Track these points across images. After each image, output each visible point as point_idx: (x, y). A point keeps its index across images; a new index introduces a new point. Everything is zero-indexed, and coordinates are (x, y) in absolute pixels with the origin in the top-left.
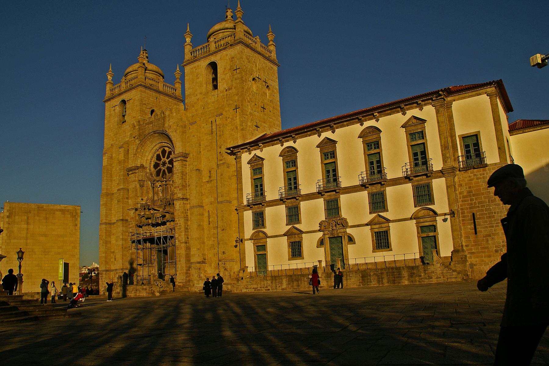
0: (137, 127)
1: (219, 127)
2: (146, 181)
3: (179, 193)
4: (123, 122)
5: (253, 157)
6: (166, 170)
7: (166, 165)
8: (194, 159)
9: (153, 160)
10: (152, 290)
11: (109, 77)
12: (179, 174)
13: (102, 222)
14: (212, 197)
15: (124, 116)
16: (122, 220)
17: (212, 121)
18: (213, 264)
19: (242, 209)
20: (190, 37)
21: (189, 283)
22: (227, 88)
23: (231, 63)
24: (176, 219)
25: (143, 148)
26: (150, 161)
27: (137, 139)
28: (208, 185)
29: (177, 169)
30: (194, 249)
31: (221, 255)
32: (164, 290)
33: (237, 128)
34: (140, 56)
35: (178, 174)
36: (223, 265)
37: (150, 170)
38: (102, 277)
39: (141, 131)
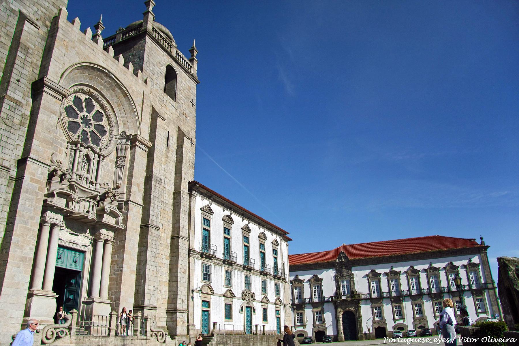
17: (169, 132)
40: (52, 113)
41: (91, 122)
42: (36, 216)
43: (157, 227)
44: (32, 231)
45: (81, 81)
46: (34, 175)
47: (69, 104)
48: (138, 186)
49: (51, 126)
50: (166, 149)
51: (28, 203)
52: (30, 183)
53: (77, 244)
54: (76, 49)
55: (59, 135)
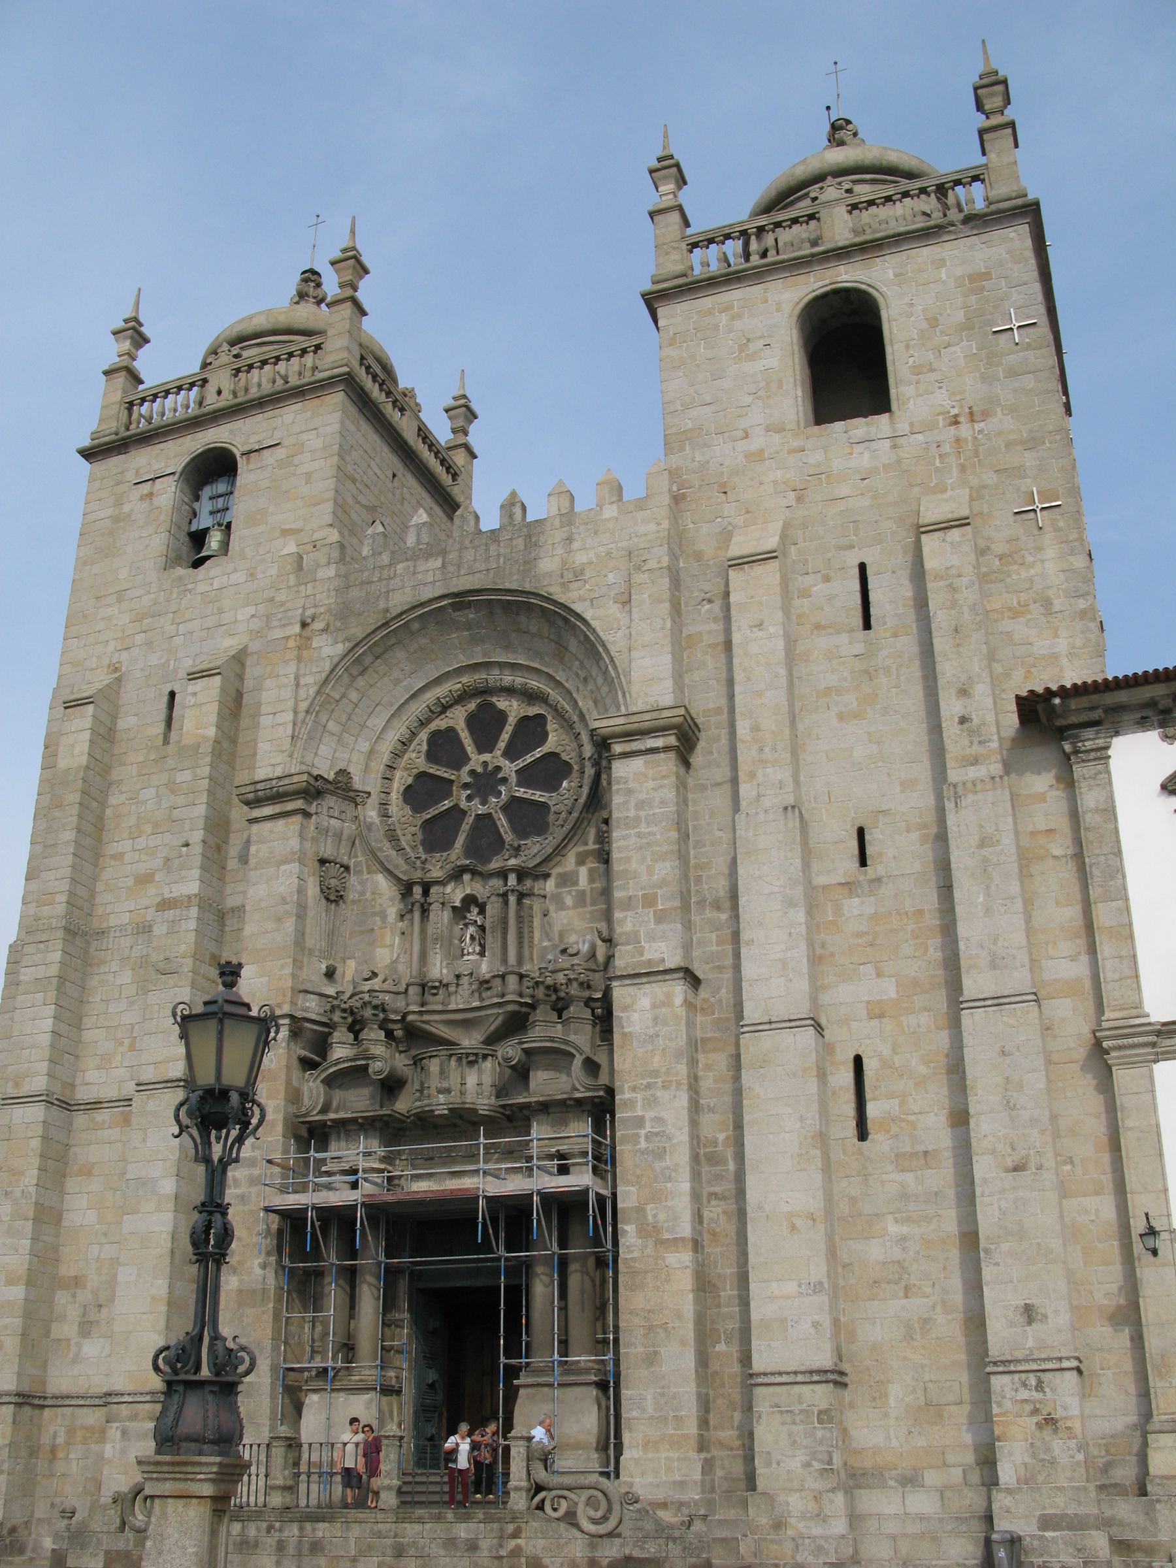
0: (331, 572)
1: (942, 583)
2: (359, 872)
3: (652, 938)
4: (197, 564)
6: (502, 822)
7: (503, 789)
8: (761, 750)
9: (403, 762)
10: (516, 1552)
12: (654, 829)
13: (17, 1085)
15: (198, 538)
17: (862, 567)
18: (895, 1391)
19: (1145, 1045)
21: (732, 1514)
22: (955, 411)
23: (973, 298)
24: (627, 1095)
25: (361, 682)
26: (386, 758)
27: (325, 630)
28: (855, 908)
29: (642, 796)
30: (774, 1285)
31: (1012, 1324)
32: (636, 1553)
33: (1047, 603)
35: (648, 824)
36: (1024, 1394)
37: (385, 815)
39: (355, 593)
41: (500, 776)
43: (790, 1021)
47: (415, 771)
48: (649, 901)
49: (284, 901)
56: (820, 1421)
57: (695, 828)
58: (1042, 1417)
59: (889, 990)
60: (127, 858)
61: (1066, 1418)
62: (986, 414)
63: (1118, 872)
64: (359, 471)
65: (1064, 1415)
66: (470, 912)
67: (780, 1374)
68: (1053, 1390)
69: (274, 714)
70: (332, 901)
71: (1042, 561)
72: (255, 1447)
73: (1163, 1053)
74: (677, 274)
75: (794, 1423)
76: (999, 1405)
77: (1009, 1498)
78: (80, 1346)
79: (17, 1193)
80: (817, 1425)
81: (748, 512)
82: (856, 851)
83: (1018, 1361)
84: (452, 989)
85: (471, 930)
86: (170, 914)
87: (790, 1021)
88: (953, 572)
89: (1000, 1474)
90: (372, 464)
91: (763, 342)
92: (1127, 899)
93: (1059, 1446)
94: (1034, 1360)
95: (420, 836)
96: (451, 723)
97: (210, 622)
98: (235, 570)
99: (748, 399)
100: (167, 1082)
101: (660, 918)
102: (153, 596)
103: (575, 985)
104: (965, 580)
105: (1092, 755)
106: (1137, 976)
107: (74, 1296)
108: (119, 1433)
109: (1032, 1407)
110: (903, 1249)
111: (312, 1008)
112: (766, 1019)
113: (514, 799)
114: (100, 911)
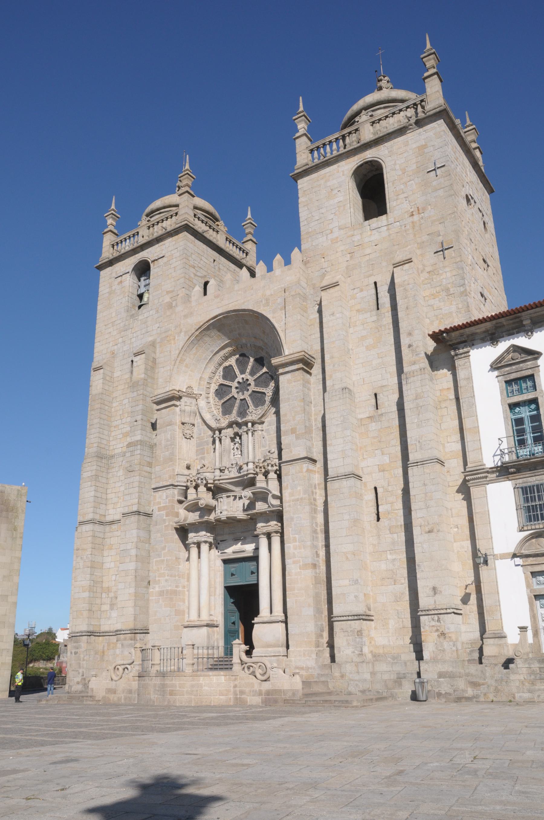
1: (402, 288)
4: (140, 307)
5: (507, 351)
8: (334, 366)
9: (214, 380)
11: (110, 221)
14: (383, 454)
16: (138, 513)
17: (375, 283)
20: (306, 122)
22: (412, 210)
26: (207, 380)
28: (373, 426)
34: (186, 172)
36: (433, 623)
38: (78, 648)
40: (168, 426)
41: (248, 383)
42: (167, 544)
43: (345, 475)
44: (165, 562)
45: (212, 352)
46: (159, 503)
47: (218, 384)
48: (293, 431)
50: (375, 318)
51: (159, 535)
52: (159, 513)
53: (244, 551)
54: (184, 330)
55: (204, 434)
56: (358, 635)
57: (314, 399)
58: (439, 633)
59: (386, 459)
60: (120, 427)
61: (449, 633)
62: (424, 209)
63: (473, 405)
64: (196, 262)
65: (448, 631)
66: (236, 438)
67: (343, 616)
68: (444, 622)
69: (164, 367)
70: (188, 439)
71: (446, 272)
72: (165, 649)
73: (490, 481)
74: (305, 164)
75: (348, 636)
76: (424, 628)
77: (427, 665)
78: (110, 613)
79: (85, 557)
80: (356, 636)
81: (332, 265)
82: (374, 403)
83: (430, 610)
84: (230, 469)
85: (237, 445)
86: (131, 449)
87: (345, 475)
88: (406, 283)
89: (424, 655)
90: (203, 258)
91: (337, 190)
92: (477, 416)
93: (446, 645)
94: (436, 610)
95: (221, 410)
96: (231, 363)
97: (144, 331)
98: (152, 310)
99: (332, 216)
100: (132, 513)
101: (297, 438)
102: (124, 323)
103: (270, 465)
104: (411, 286)
105: (463, 355)
106: (481, 448)
107: (108, 595)
108: (121, 645)
109: (436, 628)
110: (394, 565)
111: (182, 481)
112: (336, 476)
113: (253, 391)
114: (111, 448)
